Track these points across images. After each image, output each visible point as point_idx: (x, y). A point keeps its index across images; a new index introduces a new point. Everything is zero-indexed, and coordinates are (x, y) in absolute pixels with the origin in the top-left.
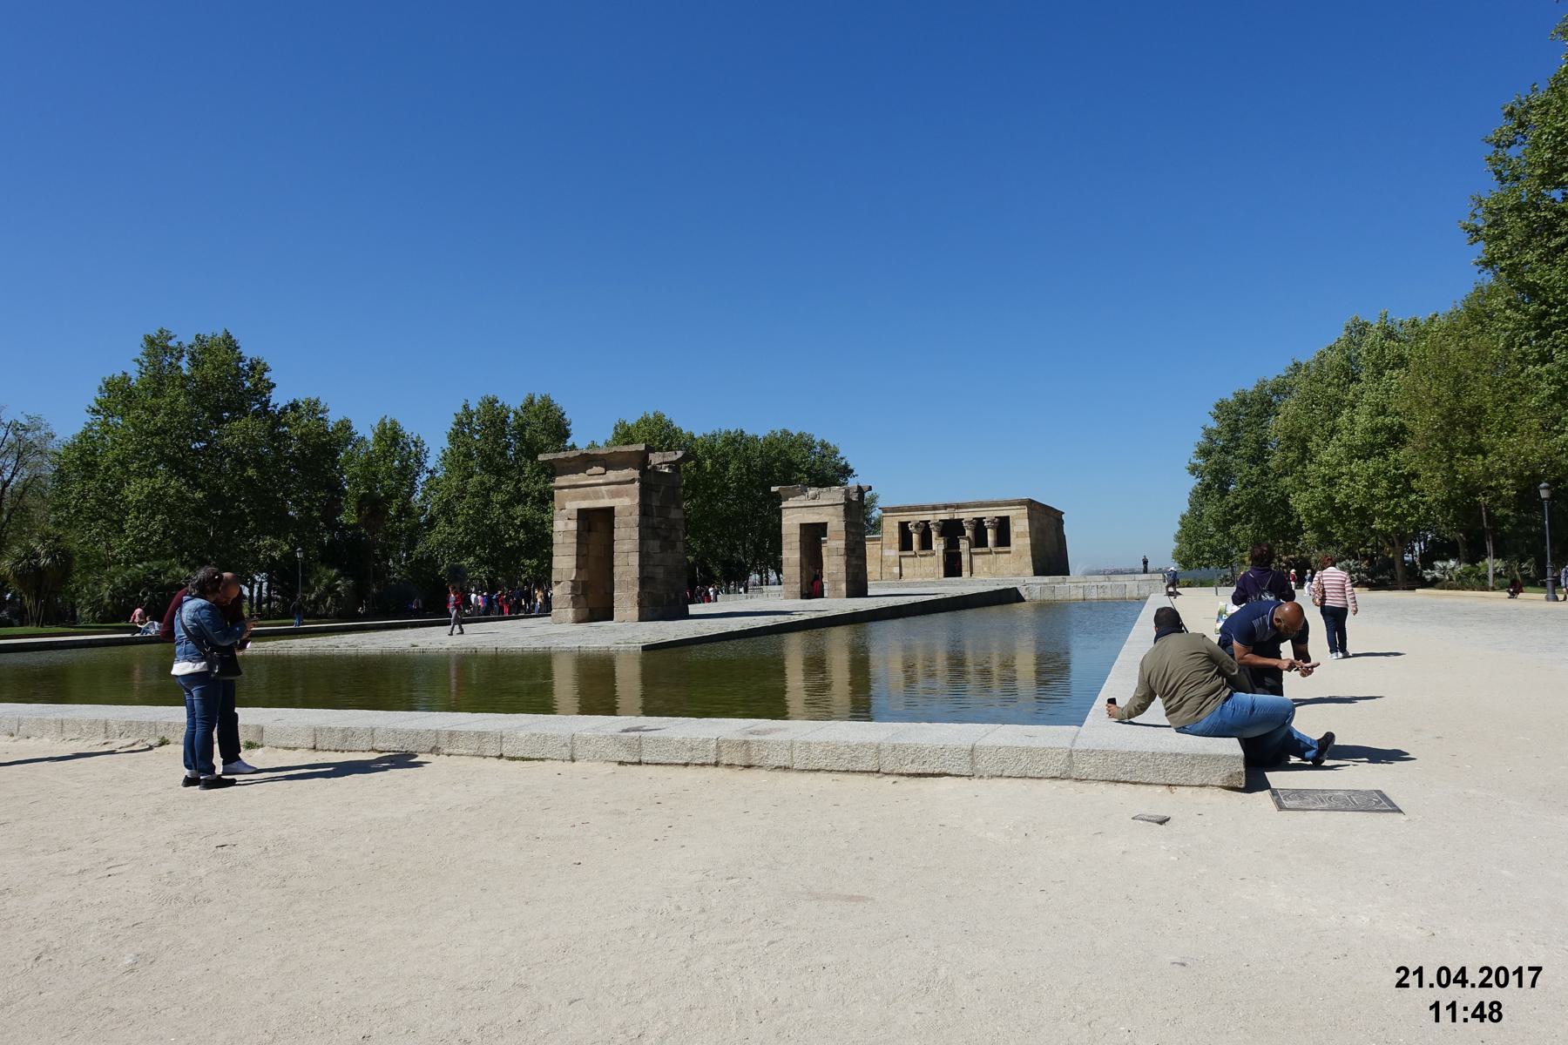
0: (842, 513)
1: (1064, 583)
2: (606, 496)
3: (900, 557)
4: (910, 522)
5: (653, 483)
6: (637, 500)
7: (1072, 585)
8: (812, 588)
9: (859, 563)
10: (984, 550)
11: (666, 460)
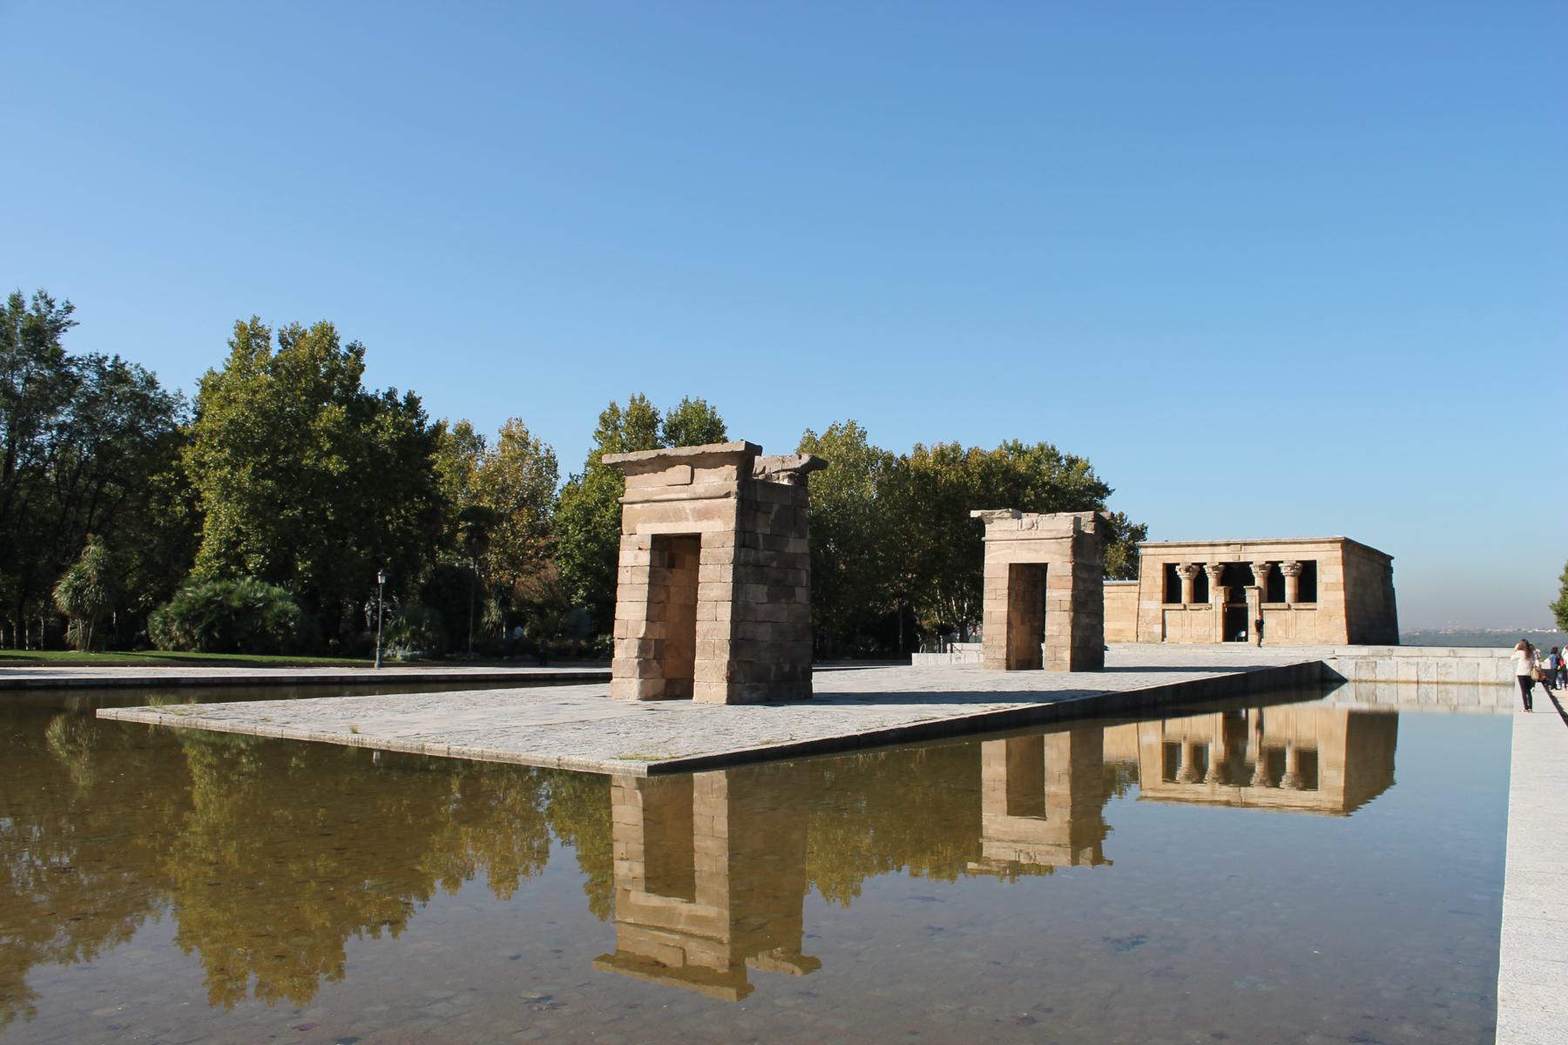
0: (1069, 551)
1: (1390, 657)
2: (690, 517)
3: (1164, 611)
4: (1178, 564)
5: (759, 500)
6: (732, 525)
7: (1398, 659)
8: (1026, 656)
9: (1094, 622)
10: (1279, 605)
11: (785, 467)
